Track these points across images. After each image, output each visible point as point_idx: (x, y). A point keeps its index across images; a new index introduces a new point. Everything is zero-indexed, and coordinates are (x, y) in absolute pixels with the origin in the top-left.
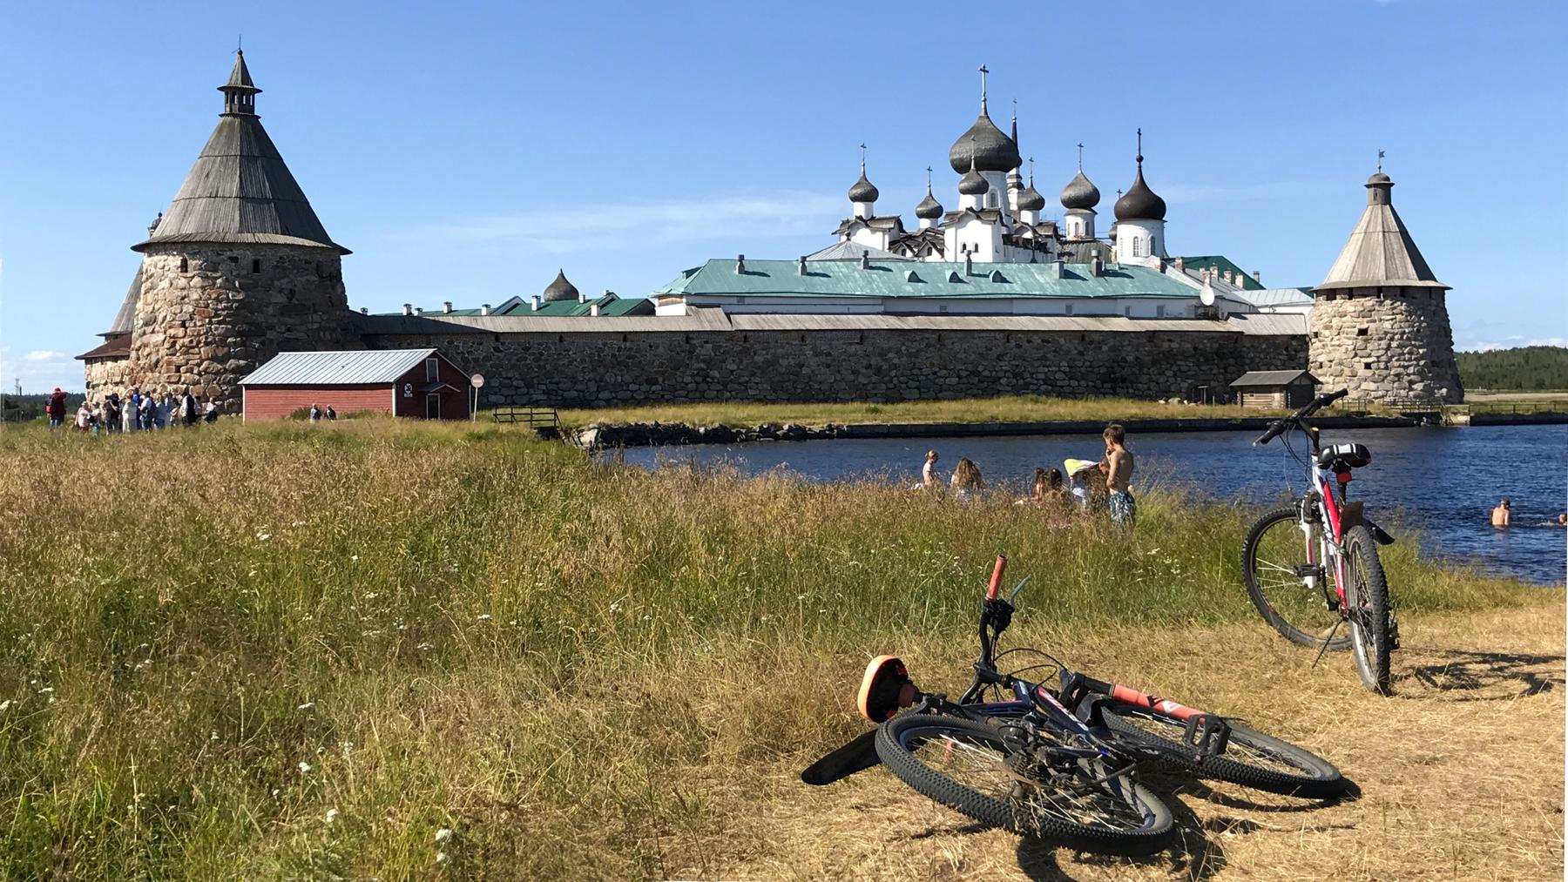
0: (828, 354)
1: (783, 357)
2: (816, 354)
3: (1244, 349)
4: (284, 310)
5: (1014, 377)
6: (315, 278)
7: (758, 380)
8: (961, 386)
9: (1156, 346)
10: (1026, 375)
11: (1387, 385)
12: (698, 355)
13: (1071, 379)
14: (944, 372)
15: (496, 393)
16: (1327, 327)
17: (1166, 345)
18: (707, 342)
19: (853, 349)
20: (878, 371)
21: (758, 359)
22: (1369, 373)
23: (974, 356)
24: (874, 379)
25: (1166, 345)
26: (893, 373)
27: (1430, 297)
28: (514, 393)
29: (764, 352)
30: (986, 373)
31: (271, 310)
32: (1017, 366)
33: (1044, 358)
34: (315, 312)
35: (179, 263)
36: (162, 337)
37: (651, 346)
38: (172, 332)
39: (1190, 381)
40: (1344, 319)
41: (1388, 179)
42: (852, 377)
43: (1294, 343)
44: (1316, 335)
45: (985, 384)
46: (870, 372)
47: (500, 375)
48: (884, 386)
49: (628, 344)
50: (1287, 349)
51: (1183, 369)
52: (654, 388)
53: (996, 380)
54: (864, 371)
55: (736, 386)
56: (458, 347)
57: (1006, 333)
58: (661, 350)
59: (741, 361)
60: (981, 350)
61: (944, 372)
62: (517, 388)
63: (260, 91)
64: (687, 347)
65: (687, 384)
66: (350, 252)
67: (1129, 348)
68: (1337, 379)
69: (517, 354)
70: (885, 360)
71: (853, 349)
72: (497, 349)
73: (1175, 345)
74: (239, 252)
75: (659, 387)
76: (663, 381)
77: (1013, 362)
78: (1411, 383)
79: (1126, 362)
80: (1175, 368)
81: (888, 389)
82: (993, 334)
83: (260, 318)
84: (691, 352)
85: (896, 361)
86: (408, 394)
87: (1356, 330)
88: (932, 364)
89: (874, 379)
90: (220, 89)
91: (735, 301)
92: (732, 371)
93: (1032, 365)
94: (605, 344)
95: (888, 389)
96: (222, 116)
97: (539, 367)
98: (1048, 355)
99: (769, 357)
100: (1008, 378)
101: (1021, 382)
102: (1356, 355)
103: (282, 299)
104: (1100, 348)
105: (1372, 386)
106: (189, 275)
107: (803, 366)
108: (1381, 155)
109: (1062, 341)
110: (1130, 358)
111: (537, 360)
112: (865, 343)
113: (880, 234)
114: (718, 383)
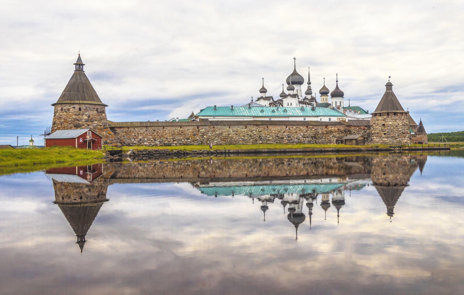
0: (236, 131)
1: (224, 132)
2: (233, 131)
3: (352, 130)
4: (86, 121)
5: (288, 137)
6: (95, 112)
7: (217, 138)
8: (273, 140)
9: (327, 129)
10: (291, 137)
11: (389, 139)
12: (201, 132)
13: (304, 137)
14: (268, 136)
15: (146, 142)
16: (374, 124)
17: (330, 128)
18: (203, 128)
19: (243, 130)
20: (250, 136)
21: (217, 133)
22: (385, 136)
23: (277, 132)
24: (249, 138)
25: (330, 128)
26: (254, 136)
27: (402, 115)
28: (151, 142)
29: (219, 131)
30: (280, 136)
31: (83, 120)
32: (289, 134)
33: (296, 132)
34: (96, 121)
35: (60, 109)
36: (56, 128)
37: (188, 130)
38: (59, 126)
39: (337, 138)
40: (379, 121)
41: (391, 83)
42: (243, 137)
43: (366, 128)
44: (372, 126)
45: (280, 139)
46: (248, 136)
47: (147, 137)
48: (252, 140)
49: (182, 129)
50: (364, 130)
51: (335, 135)
52: (188, 141)
53: (282, 138)
54: (246, 136)
55: (211, 140)
56: (136, 130)
57: (286, 126)
58: (190, 130)
59: (212, 133)
60: (279, 130)
61: (268, 136)
62: (152, 141)
63: (84, 65)
64: (197, 130)
65: (198, 139)
66: (107, 106)
67: (320, 129)
68: (377, 138)
69: (152, 132)
70: (252, 133)
71: (243, 130)
72: (146, 131)
73: (333, 129)
74: (75, 106)
75: (190, 140)
76: (191, 139)
77: (288, 133)
78: (396, 138)
79: (319, 133)
80: (332, 135)
81: (253, 141)
82: (282, 126)
83: (80, 122)
84: (199, 131)
85: (255, 133)
86: (81, 141)
87: (382, 124)
88: (265, 134)
89: (249, 138)
90: (74, 64)
91: (212, 118)
92: (210, 136)
93: (293, 134)
94: (175, 129)
95: (253, 141)
96: (74, 71)
97: (158, 135)
98: (298, 132)
99: (220, 132)
100: (286, 137)
101: (290, 139)
102: (382, 131)
103: (86, 118)
104: (312, 130)
105: (386, 139)
106: (63, 112)
107: (229, 135)
108: (390, 77)
109: (301, 128)
110: (320, 132)
111: (157, 133)
112: (247, 128)
113: (267, 101)
114: (206, 139)
